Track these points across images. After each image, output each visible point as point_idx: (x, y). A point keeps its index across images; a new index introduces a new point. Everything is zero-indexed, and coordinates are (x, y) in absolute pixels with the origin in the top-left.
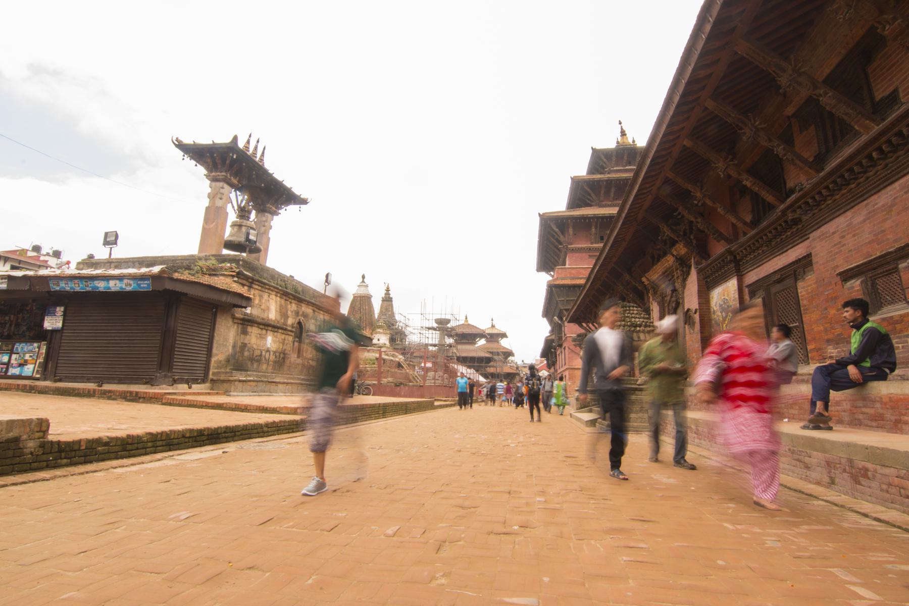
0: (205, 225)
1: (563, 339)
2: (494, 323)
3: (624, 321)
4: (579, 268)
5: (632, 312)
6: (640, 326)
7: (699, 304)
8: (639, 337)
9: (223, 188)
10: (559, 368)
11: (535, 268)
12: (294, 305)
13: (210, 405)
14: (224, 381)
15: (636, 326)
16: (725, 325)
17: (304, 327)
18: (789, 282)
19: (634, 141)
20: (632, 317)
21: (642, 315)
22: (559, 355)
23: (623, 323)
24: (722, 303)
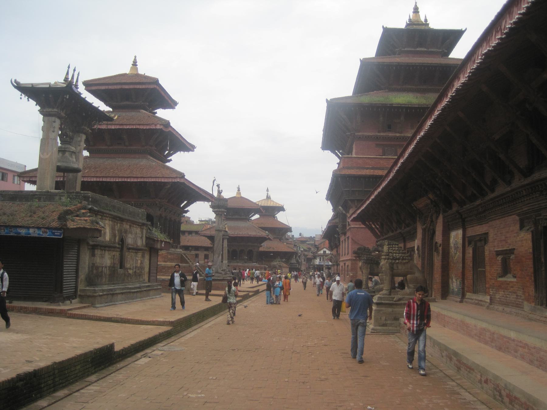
0: (42, 156)
1: (348, 228)
2: (270, 193)
3: (388, 255)
4: (366, 158)
5: (394, 249)
6: (399, 259)
7: (442, 240)
8: (398, 267)
9: (54, 122)
10: (342, 255)
11: (320, 145)
12: (119, 225)
13: (102, 318)
14: (89, 296)
15: (396, 259)
16: (455, 259)
17: (124, 241)
18: (483, 242)
19: (426, 20)
20: (394, 253)
21: (401, 251)
22: (342, 241)
23: (387, 257)
24: (455, 243)
